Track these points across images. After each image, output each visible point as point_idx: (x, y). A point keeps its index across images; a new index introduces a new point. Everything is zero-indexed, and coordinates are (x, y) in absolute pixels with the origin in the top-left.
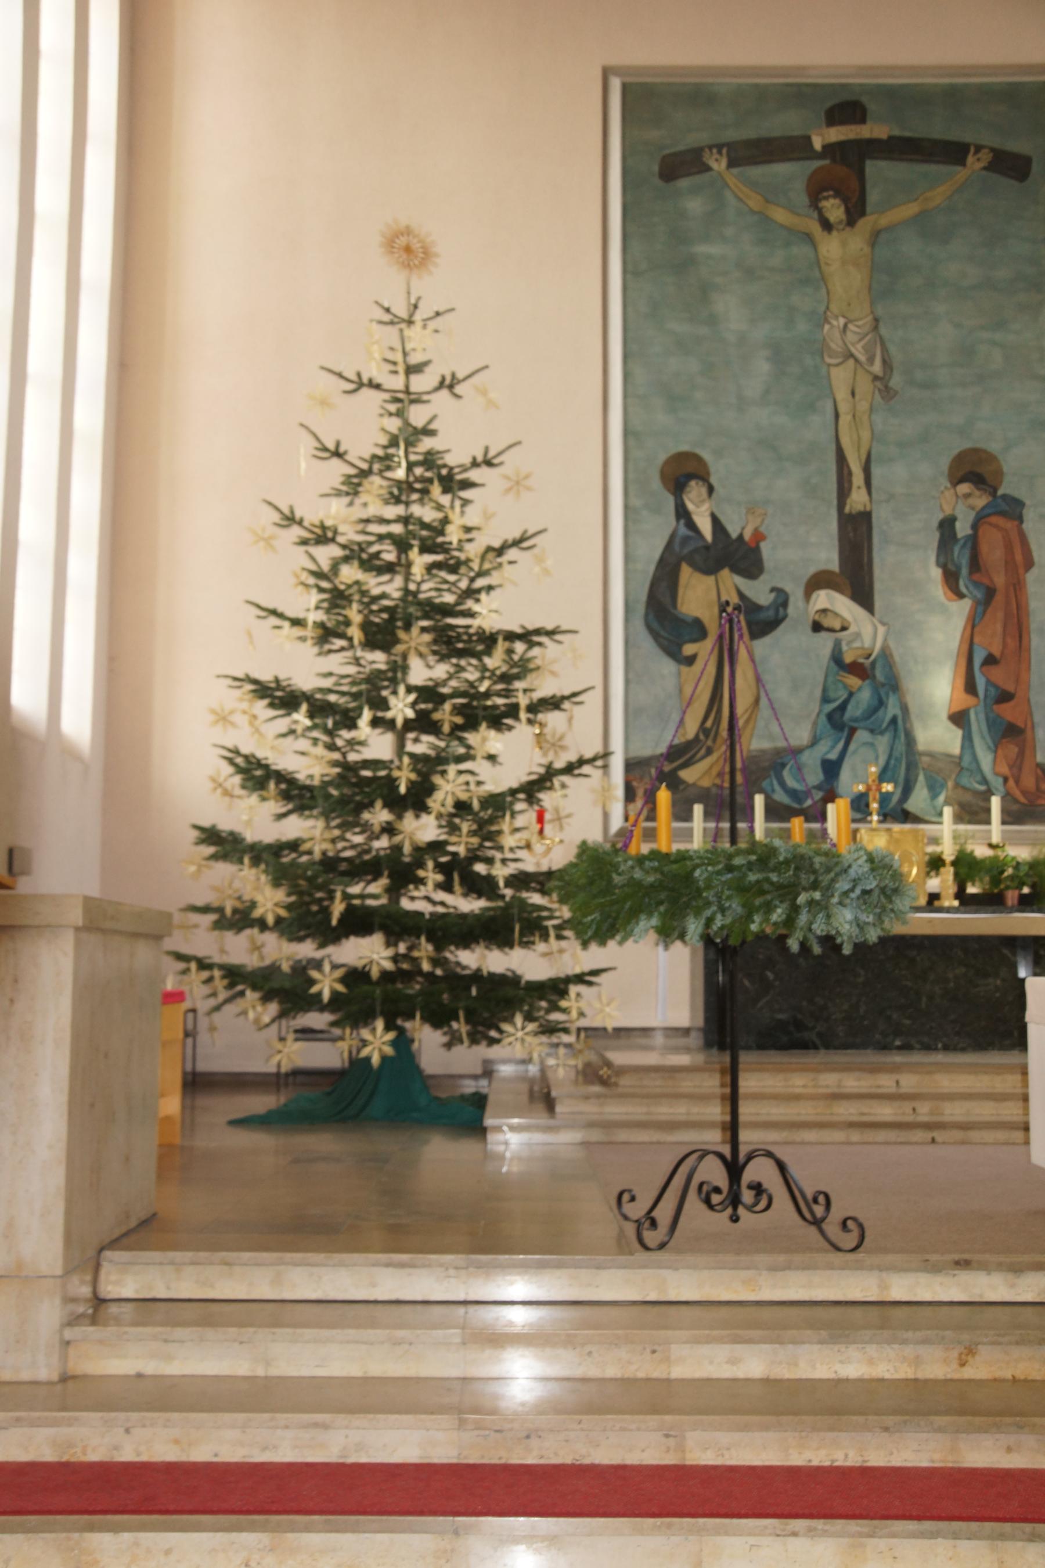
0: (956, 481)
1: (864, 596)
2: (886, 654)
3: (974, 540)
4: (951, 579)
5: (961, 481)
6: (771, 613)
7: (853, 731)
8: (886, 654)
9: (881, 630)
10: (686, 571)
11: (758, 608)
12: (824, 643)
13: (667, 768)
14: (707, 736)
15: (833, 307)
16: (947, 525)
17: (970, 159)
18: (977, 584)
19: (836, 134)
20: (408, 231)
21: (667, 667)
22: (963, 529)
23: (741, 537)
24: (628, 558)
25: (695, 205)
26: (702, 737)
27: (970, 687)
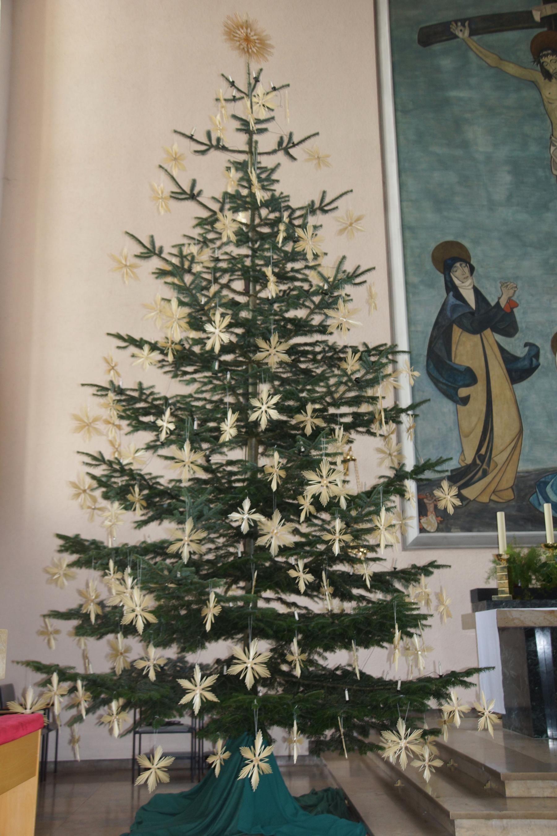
6: (526, 363)
10: (457, 331)
11: (516, 359)
14: (482, 462)
20: (247, 25)
21: (448, 406)
23: (498, 304)
24: (410, 322)
26: (478, 462)
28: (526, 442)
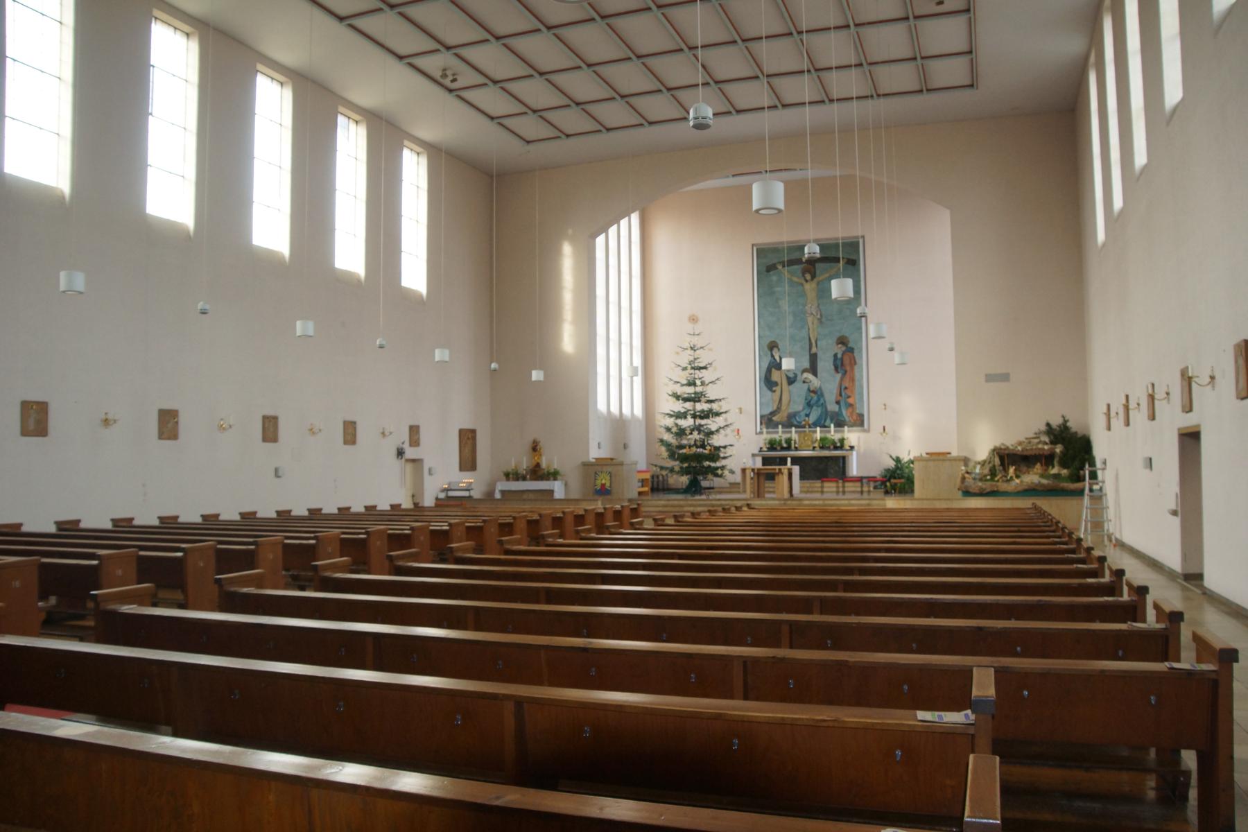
0: (838, 344)
1: (815, 374)
2: (820, 388)
3: (842, 359)
6: (793, 380)
7: (812, 407)
8: (820, 388)
9: (819, 382)
10: (773, 370)
12: (806, 386)
13: (770, 416)
16: (835, 355)
20: (693, 315)
21: (769, 393)
22: (839, 356)
24: (760, 367)
25: (774, 278)
27: (841, 395)
28: (791, 403)
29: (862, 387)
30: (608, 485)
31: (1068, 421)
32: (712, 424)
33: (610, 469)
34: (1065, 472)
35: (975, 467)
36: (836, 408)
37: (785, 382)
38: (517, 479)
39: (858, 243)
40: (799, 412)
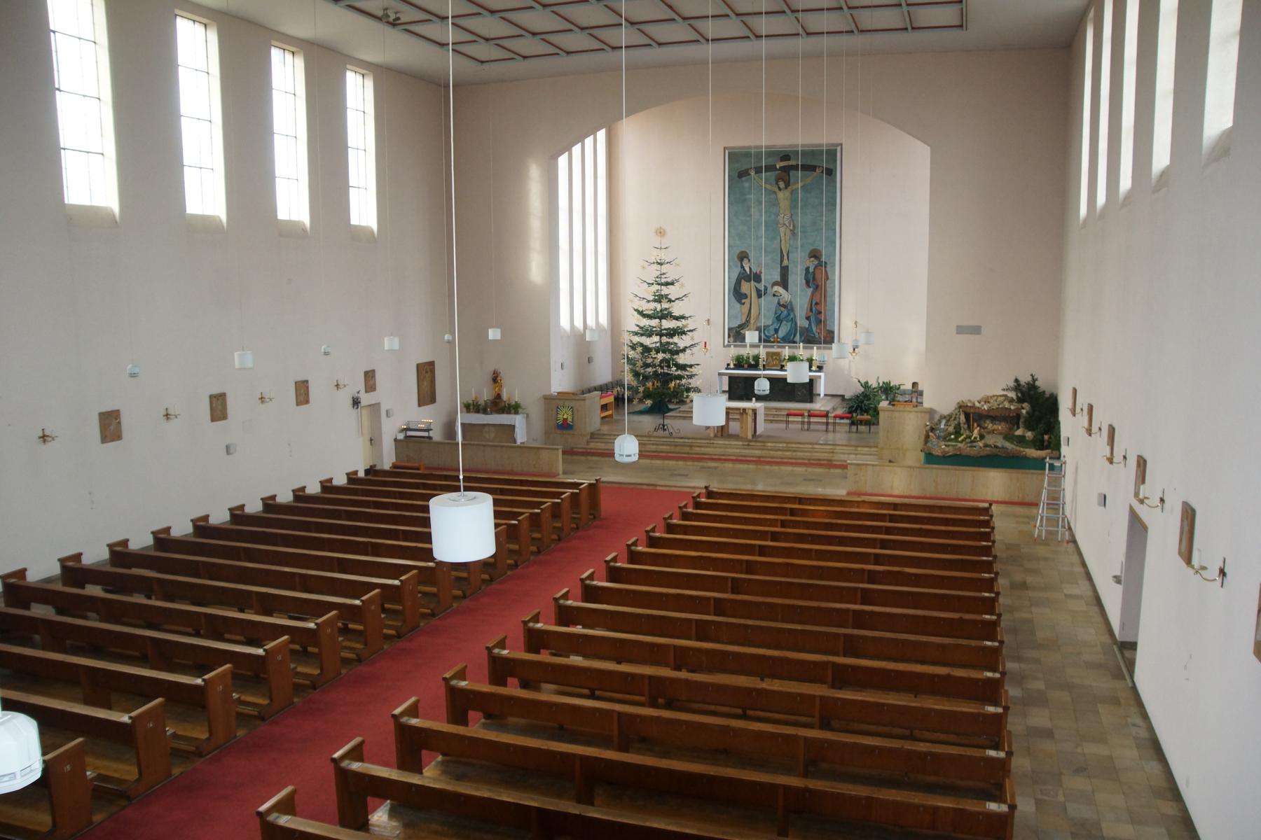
1: (786, 287)
2: (791, 302)
3: (814, 273)
4: (808, 283)
5: (812, 257)
8: (791, 302)
10: (743, 281)
12: (776, 300)
15: (781, 212)
16: (807, 269)
17: (817, 170)
18: (814, 284)
19: (783, 164)
21: (738, 305)
22: (811, 270)
24: (729, 278)
25: (746, 185)
27: (811, 310)
29: (834, 304)
30: (570, 419)
31: (1037, 380)
32: (681, 342)
33: (572, 404)
34: (1029, 435)
35: (940, 421)
36: (806, 324)
37: (754, 294)
38: (477, 411)
39: (836, 150)
40: (768, 326)
